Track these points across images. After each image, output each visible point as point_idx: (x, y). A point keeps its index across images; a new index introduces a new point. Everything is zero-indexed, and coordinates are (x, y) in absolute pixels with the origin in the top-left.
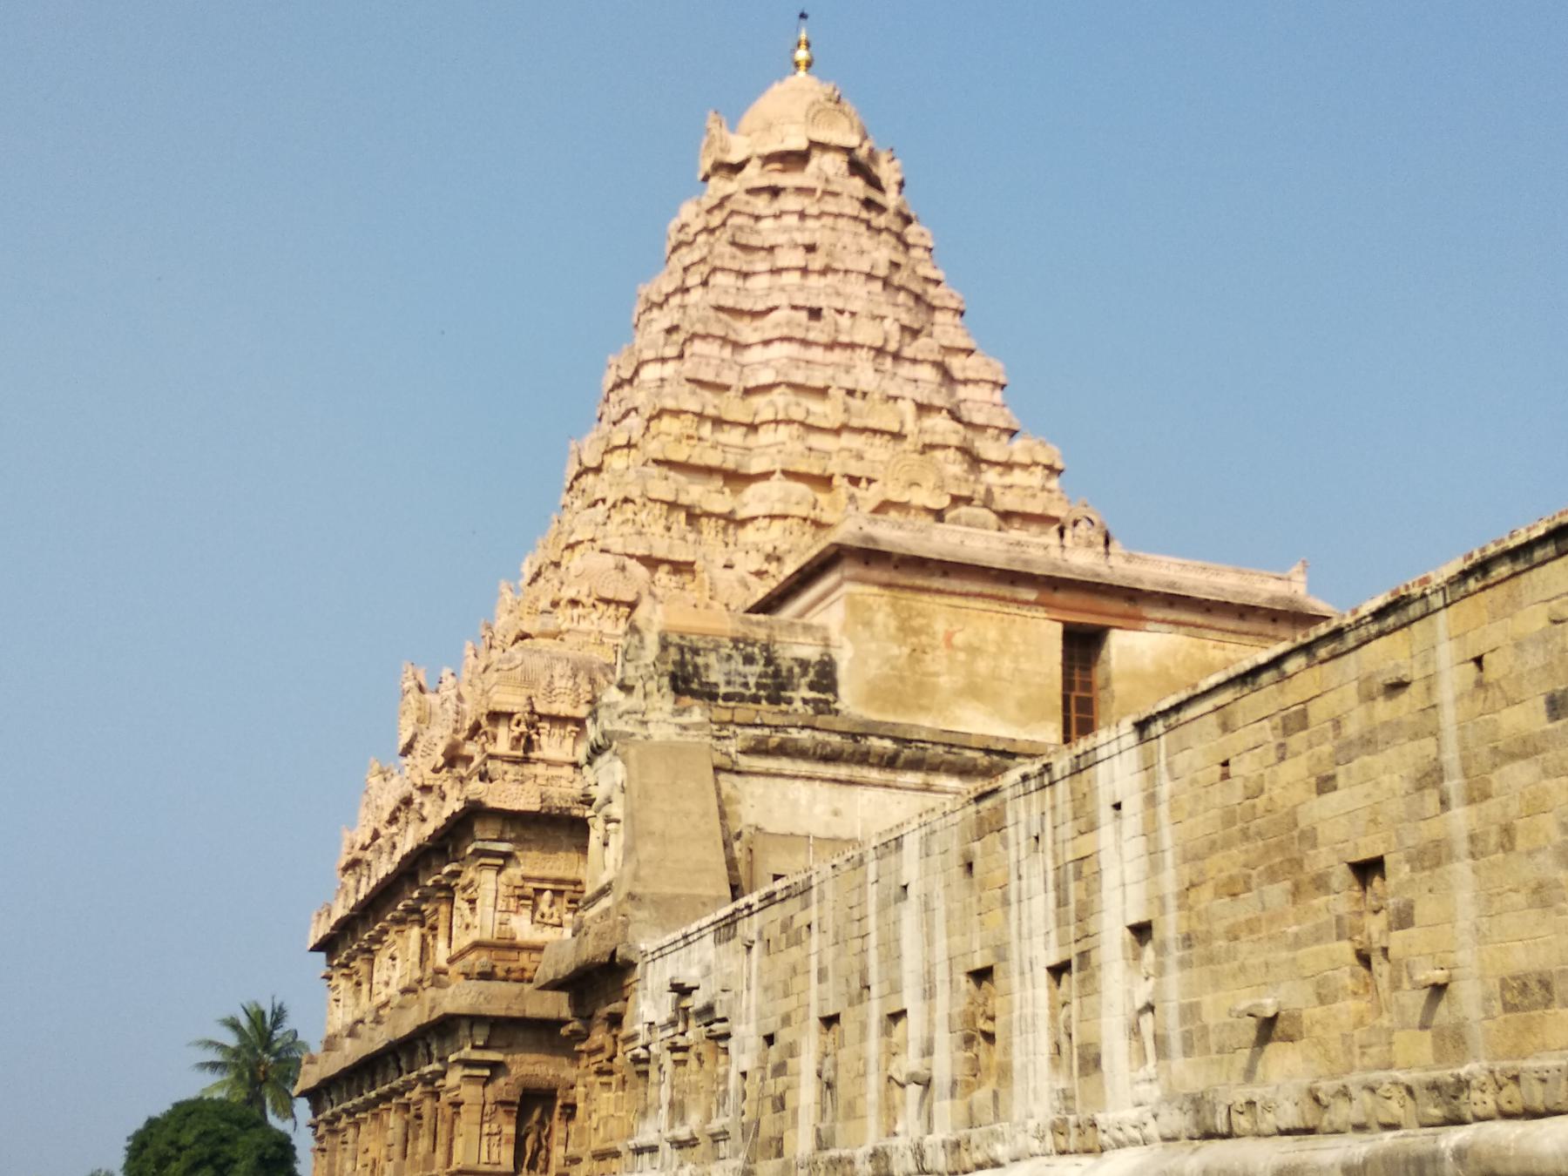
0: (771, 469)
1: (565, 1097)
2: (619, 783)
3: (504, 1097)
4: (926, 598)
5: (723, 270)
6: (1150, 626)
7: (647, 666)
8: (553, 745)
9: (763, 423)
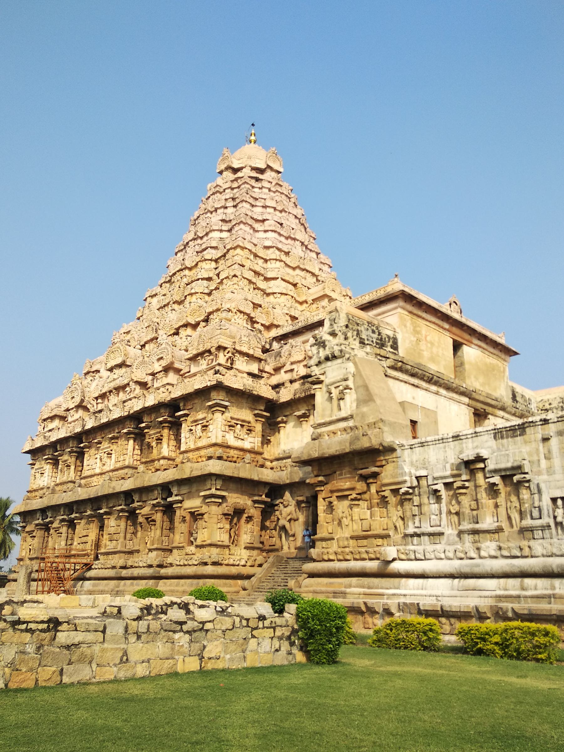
0: (277, 276)
1: (248, 513)
2: (352, 372)
3: (226, 512)
4: (420, 320)
5: (246, 201)
6: (473, 346)
7: (341, 327)
8: (241, 364)
9: (270, 260)
